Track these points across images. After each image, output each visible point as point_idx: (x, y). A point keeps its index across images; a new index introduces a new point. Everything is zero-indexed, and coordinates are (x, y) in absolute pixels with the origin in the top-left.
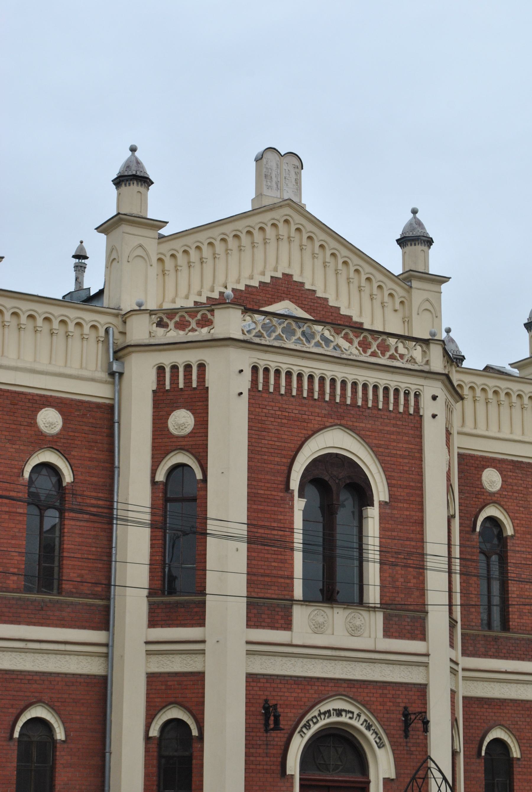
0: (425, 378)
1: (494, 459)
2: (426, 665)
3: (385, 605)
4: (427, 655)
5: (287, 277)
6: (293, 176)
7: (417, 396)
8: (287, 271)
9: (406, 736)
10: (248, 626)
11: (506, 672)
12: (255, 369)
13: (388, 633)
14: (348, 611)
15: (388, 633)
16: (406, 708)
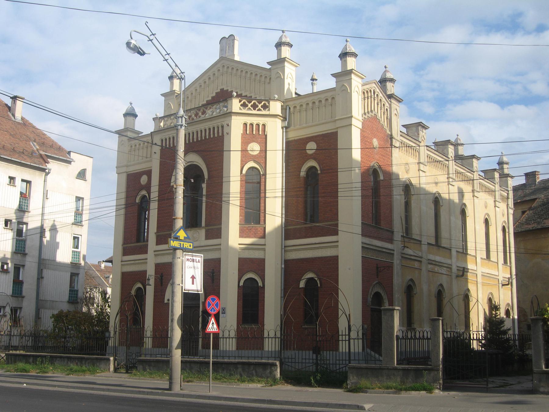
0: (225, 117)
1: (312, 137)
2: (220, 249)
3: (207, 225)
4: (220, 245)
5: (222, 90)
6: (232, 44)
7: (223, 127)
8: (222, 87)
9: (213, 282)
10: (157, 245)
11: (315, 244)
12: (162, 140)
13: (207, 237)
14: (192, 231)
15: (207, 237)
16: (213, 270)
